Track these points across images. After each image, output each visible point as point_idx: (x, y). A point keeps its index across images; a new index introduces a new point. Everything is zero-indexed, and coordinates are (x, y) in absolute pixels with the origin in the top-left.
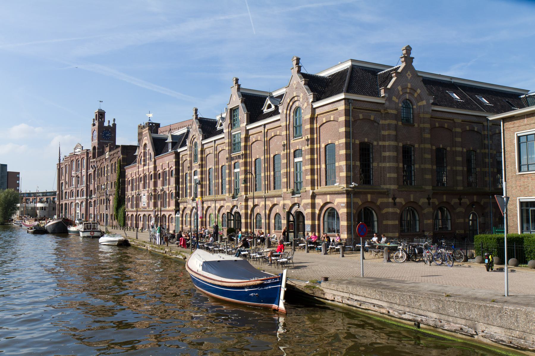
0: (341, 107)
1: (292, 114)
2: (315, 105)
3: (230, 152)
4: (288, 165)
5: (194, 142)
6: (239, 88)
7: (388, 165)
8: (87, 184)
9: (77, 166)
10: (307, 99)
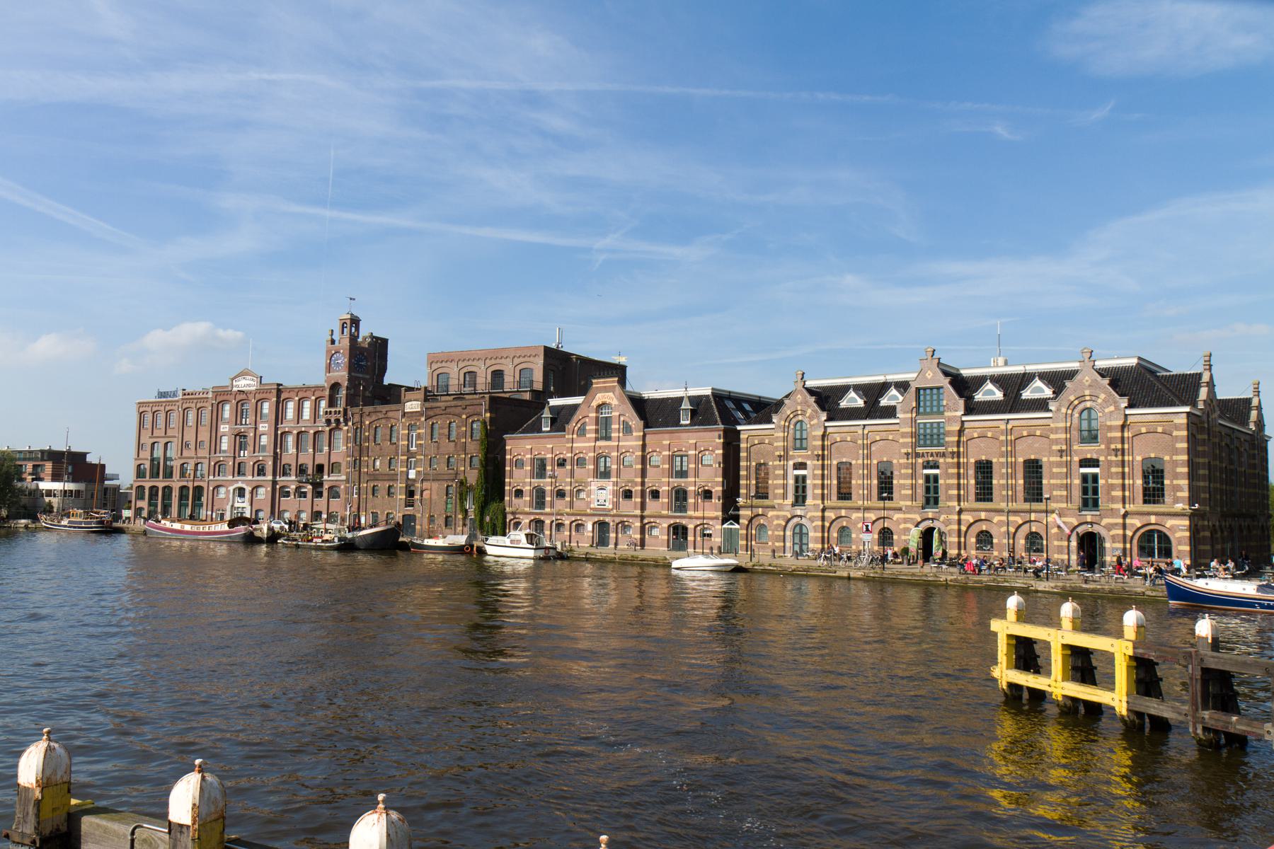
0: (1183, 420)
1: (1076, 415)
2: (1128, 412)
3: (914, 446)
4: (1068, 475)
5: (794, 421)
6: (939, 363)
7: (1202, 484)
8: (275, 453)
9: (239, 414)
10: (1115, 402)
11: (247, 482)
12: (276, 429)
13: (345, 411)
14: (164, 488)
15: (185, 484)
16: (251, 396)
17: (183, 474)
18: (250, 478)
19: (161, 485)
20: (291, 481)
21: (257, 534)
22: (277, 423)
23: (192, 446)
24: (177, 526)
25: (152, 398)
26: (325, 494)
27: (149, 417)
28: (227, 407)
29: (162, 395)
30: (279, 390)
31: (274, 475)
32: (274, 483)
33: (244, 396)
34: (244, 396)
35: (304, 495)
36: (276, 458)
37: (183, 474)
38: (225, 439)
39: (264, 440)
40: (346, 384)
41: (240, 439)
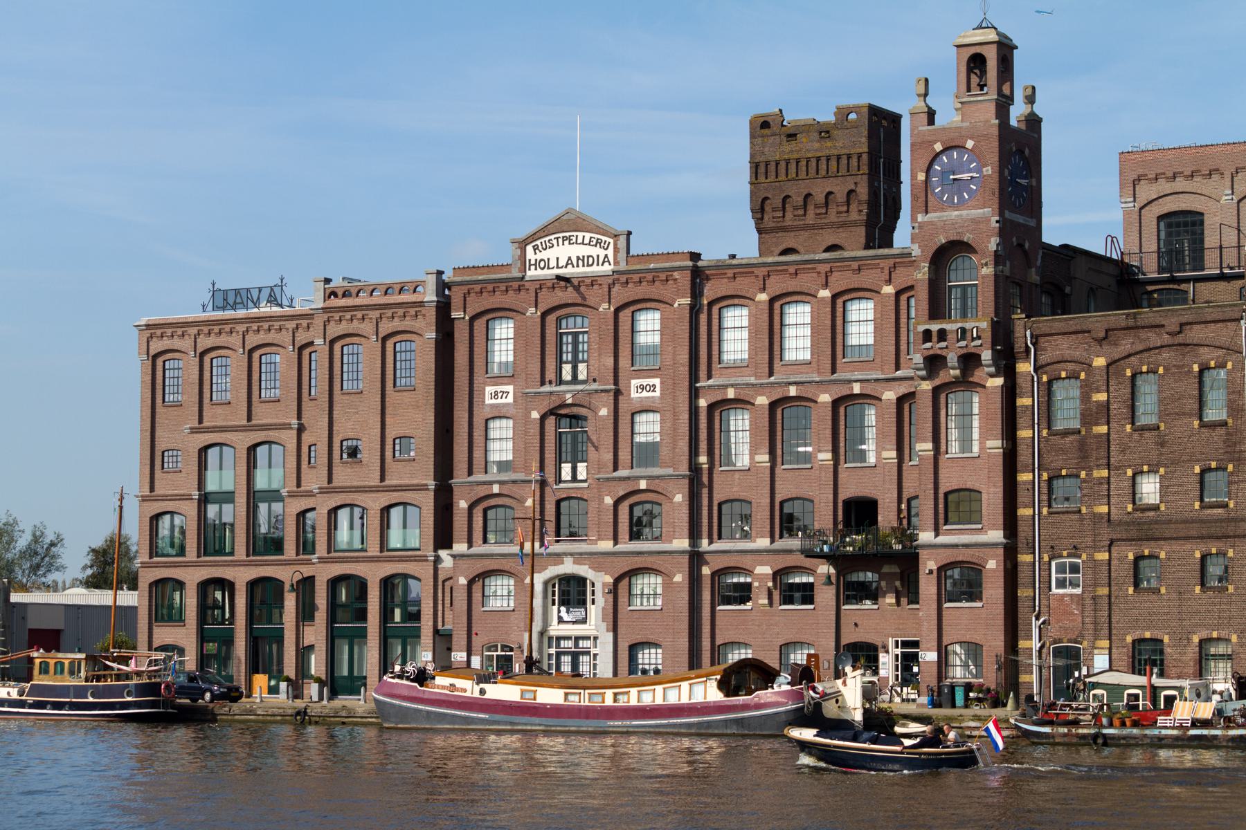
8: (694, 468)
9: (545, 349)
11: (597, 560)
12: (694, 393)
13: (1002, 335)
14: (253, 585)
15: (307, 571)
16: (592, 296)
17: (306, 546)
18: (606, 545)
19: (287, 575)
20: (756, 551)
21: (830, 709)
22: (694, 376)
23: (370, 454)
24: (469, 688)
25: (190, 304)
26: (928, 587)
27: (182, 371)
28: (504, 331)
29: (225, 298)
30: (698, 275)
31: (694, 535)
32: (696, 558)
33: (569, 295)
34: (569, 295)
35: (806, 594)
36: (696, 482)
37: (306, 546)
38: (502, 430)
39: (649, 428)
40: (993, 244)
41: (563, 427)
